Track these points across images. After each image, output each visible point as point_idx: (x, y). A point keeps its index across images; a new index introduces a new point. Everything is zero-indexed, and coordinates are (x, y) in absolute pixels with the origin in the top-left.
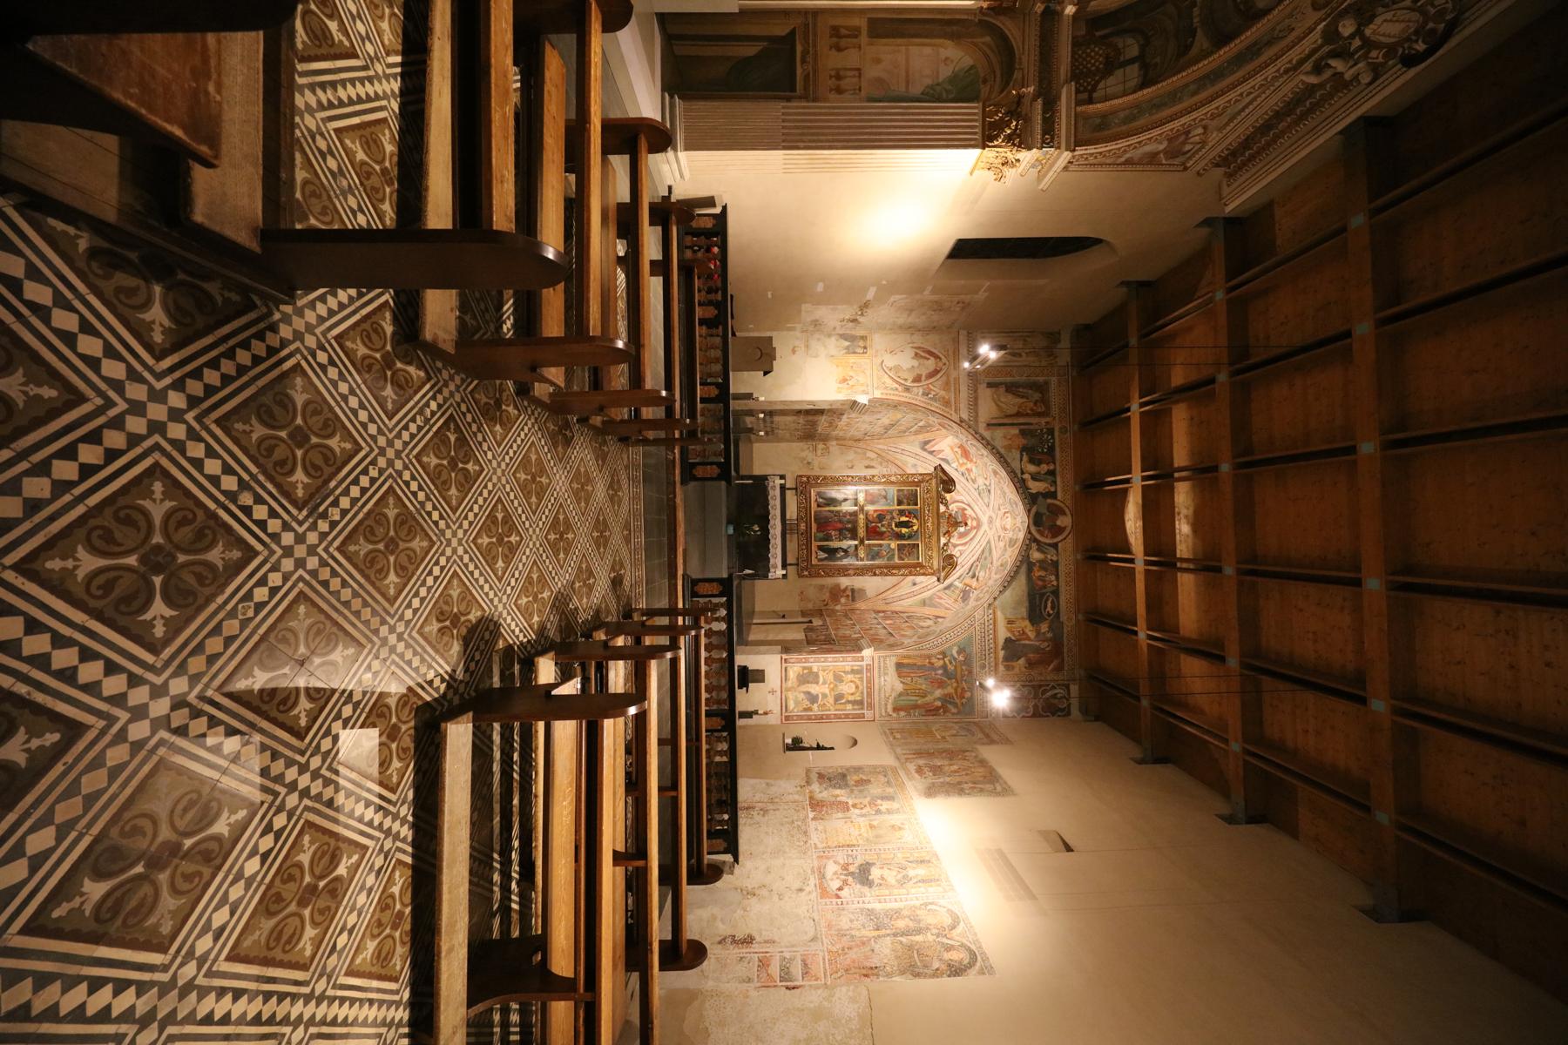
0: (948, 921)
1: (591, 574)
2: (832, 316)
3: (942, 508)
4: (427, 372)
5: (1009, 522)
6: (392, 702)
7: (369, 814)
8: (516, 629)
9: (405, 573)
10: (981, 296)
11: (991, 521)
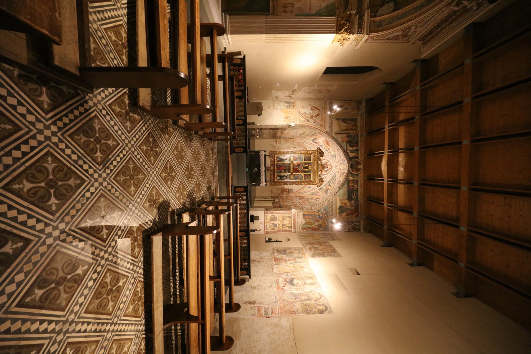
0: (319, 297)
1: (200, 185)
2: (282, 95)
3: (319, 162)
4: (141, 117)
5: (342, 167)
6: (135, 229)
7: (129, 266)
8: (175, 204)
9: (137, 186)
10: (335, 87)
11: (336, 166)
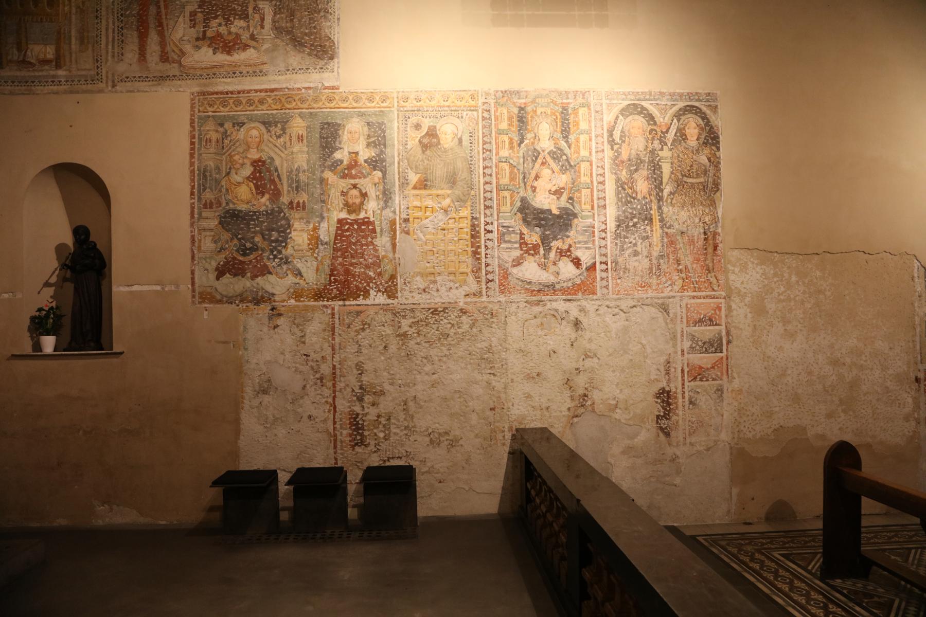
0: (639, 122)
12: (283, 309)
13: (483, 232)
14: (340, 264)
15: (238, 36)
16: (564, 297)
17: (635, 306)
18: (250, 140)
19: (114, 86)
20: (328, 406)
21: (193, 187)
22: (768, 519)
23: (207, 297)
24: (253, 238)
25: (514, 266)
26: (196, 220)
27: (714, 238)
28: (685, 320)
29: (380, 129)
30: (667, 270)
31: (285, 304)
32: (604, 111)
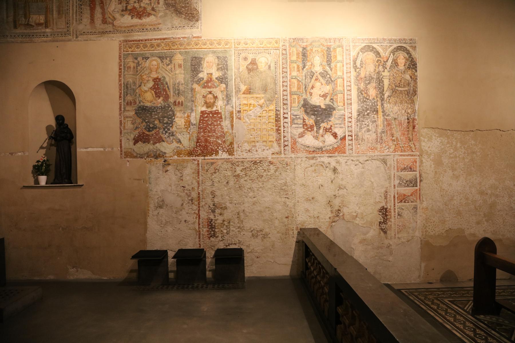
0: (371, 55)
12: (170, 161)
13: (282, 118)
14: (202, 136)
15: (145, 8)
16: (327, 155)
17: (367, 160)
18: (152, 67)
19: (76, 38)
20: (195, 215)
21: (121, 93)
22: (442, 281)
23: (129, 154)
24: (154, 121)
25: (300, 137)
26: (122, 112)
27: (413, 122)
28: (396, 168)
29: (224, 60)
30: (386, 140)
31: (172, 158)
32: (351, 50)
